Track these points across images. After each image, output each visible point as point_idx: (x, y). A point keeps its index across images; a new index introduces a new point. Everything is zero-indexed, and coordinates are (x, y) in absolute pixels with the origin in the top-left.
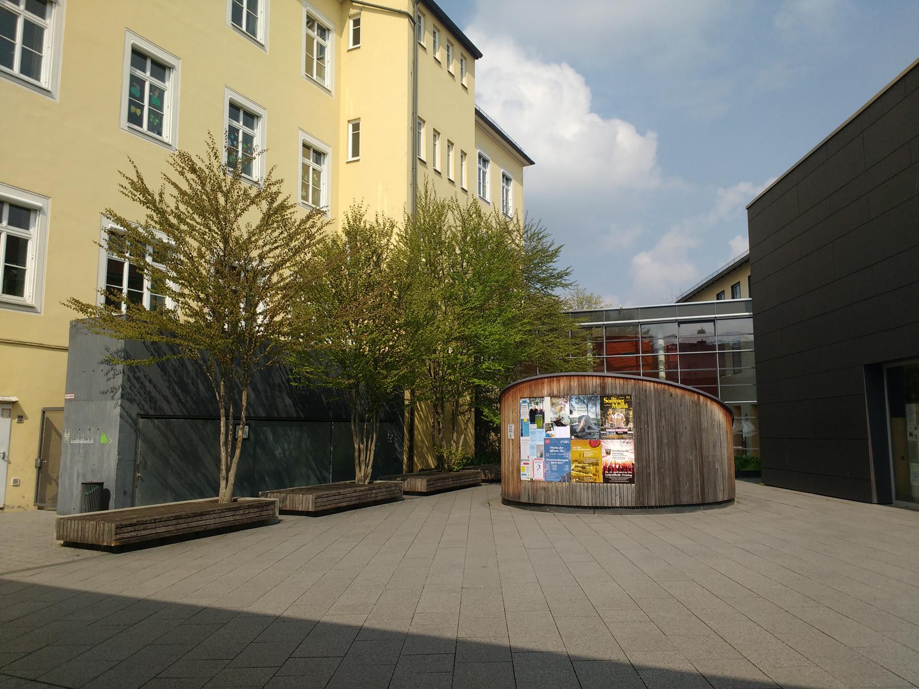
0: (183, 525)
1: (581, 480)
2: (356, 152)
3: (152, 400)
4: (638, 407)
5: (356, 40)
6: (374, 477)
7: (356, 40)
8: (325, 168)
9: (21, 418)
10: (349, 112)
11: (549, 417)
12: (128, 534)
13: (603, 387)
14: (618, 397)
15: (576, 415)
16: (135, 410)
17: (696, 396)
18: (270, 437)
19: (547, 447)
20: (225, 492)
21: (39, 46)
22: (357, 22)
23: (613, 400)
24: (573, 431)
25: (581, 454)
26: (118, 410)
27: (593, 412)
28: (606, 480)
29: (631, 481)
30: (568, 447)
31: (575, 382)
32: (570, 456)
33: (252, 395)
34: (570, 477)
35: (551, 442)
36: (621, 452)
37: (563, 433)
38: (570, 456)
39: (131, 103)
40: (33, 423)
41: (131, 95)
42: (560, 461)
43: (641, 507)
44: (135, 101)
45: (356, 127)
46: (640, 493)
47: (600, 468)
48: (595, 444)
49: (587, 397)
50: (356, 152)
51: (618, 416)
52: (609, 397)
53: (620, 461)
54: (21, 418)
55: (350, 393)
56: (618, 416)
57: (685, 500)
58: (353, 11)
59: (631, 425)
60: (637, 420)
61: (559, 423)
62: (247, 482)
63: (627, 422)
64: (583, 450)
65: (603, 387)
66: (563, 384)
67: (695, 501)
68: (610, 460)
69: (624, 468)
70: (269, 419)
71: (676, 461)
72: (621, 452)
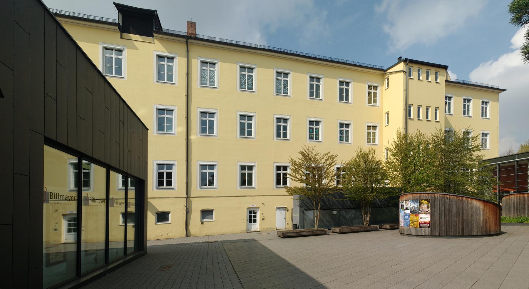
0: (298, 234)
1: (412, 226)
2: (388, 123)
3: (308, 207)
4: (433, 203)
5: (388, 86)
6: (370, 224)
7: (388, 86)
8: (377, 131)
9: (288, 211)
10: (385, 111)
11: (405, 207)
12: (285, 235)
13: (420, 197)
14: (425, 200)
15: (411, 206)
16: (303, 209)
17: (461, 198)
18: (345, 213)
19: (404, 216)
20: (316, 227)
21: (286, 130)
22: (388, 80)
23: (423, 201)
24: (411, 211)
25: (413, 219)
26: (299, 210)
27: (416, 205)
28: (420, 227)
29: (429, 227)
30: (409, 216)
31: (411, 196)
32: (409, 219)
33: (323, 204)
34: (409, 226)
35: (405, 215)
36: (426, 218)
37: (408, 212)
38: (409, 219)
39: (310, 135)
40: (290, 211)
41: (310, 132)
42: (407, 221)
43: (432, 235)
44: (311, 133)
45: (388, 114)
46: (431, 231)
47: (418, 223)
48: (417, 215)
49: (415, 201)
50: (388, 123)
51: (425, 206)
52: (422, 200)
53: (425, 221)
54: (288, 211)
55: (347, 203)
56: (425, 206)
57: (452, 234)
58: (386, 76)
59: (429, 209)
60: (432, 207)
61: (407, 209)
62: (371, 222)
63: (428, 208)
64: (413, 217)
65: (420, 197)
66: (408, 196)
67: (458, 234)
68: (421, 220)
69: (426, 223)
70: (343, 209)
71: (449, 221)
72: (426, 218)
